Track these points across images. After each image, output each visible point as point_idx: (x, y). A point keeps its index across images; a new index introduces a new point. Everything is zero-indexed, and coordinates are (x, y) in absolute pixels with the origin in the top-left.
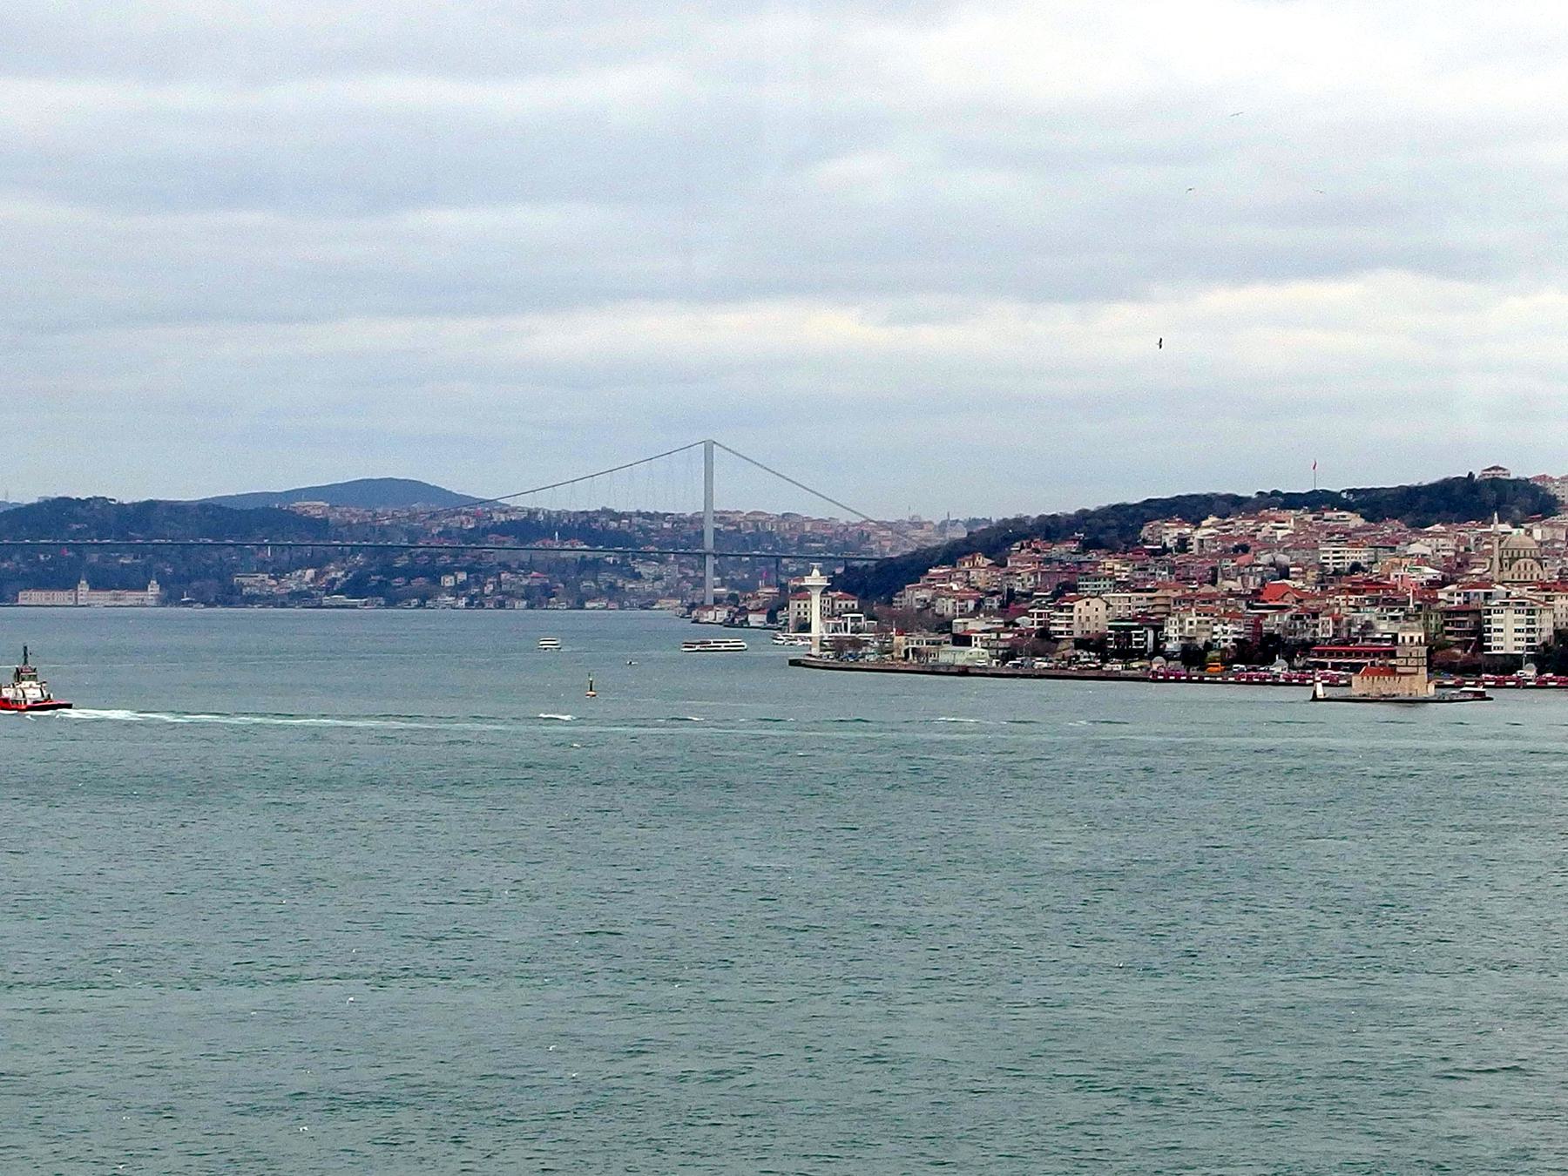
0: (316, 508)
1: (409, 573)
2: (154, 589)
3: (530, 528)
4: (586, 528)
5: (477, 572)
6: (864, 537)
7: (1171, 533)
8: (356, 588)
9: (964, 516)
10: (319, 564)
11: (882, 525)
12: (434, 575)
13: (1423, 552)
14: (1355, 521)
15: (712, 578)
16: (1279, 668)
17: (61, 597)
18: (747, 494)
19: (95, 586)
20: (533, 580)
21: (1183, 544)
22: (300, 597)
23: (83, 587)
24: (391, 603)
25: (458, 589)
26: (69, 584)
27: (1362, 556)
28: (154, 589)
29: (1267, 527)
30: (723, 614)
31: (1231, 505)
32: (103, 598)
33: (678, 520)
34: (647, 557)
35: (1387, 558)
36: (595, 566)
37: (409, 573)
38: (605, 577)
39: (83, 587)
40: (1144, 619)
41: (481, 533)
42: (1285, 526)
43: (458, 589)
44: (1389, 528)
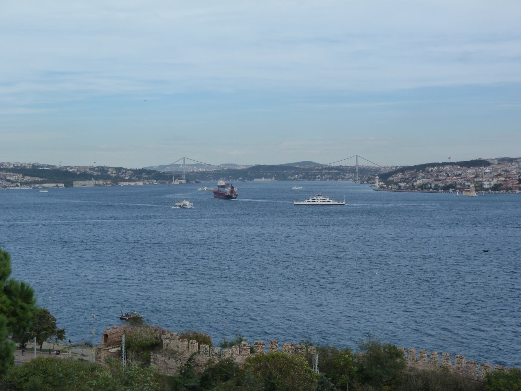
0: (297, 166)
1: (311, 175)
2: (273, 178)
3: (330, 168)
4: (337, 168)
5: (322, 175)
6: (380, 169)
7: (430, 169)
8: (304, 178)
9: (394, 166)
10: (298, 174)
11: (382, 167)
12: (315, 176)
14: (459, 167)
15: (357, 176)
16: (451, 190)
17: (259, 180)
18: (362, 163)
19: (265, 178)
20: (330, 176)
21: (432, 171)
22: (295, 179)
23: (263, 178)
24: (309, 179)
25: (319, 178)
26: (261, 178)
27: (460, 172)
28: (273, 178)
29: (445, 169)
30: (359, 182)
31: (438, 165)
32: (266, 180)
33: (351, 167)
34: (347, 173)
35: (465, 173)
36: (339, 174)
37: (311, 175)
38: (341, 176)
39: (263, 178)
40: (429, 183)
41: (322, 169)
42: (448, 168)
43: (319, 178)
44: (465, 168)
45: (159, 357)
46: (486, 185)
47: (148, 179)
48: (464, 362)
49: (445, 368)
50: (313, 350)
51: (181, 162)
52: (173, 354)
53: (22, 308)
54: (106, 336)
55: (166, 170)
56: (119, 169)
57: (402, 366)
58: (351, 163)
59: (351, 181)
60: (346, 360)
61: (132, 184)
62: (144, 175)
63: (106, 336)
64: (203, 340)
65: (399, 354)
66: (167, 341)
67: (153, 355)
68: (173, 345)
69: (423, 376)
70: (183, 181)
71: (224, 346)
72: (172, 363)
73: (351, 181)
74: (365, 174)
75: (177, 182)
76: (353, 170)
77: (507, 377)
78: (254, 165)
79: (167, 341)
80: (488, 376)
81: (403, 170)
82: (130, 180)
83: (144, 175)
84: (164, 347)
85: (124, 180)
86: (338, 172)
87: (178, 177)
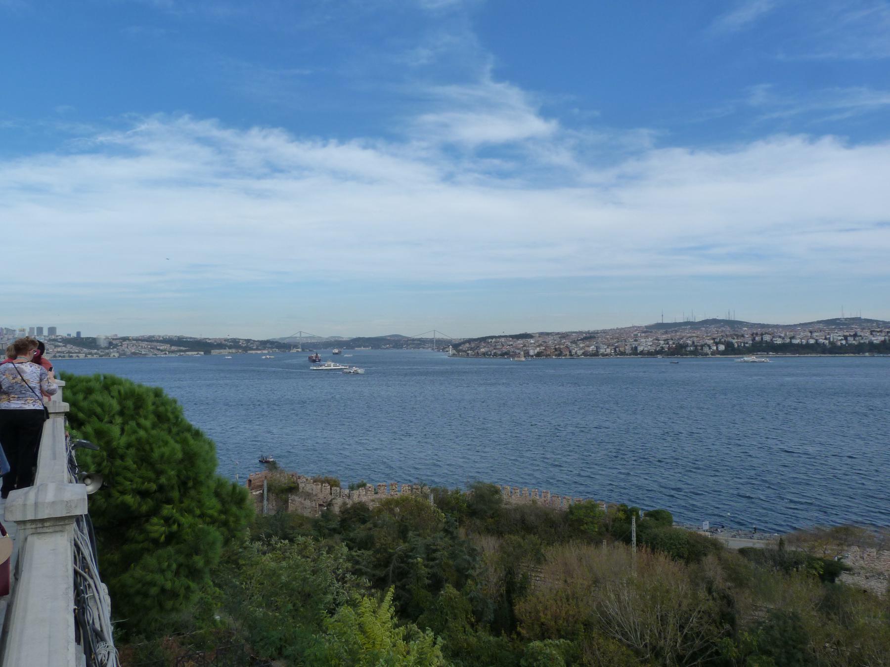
3: (414, 340)
4: (419, 340)
5: (408, 345)
8: (394, 347)
13: (520, 341)
18: (438, 336)
36: (420, 344)
42: (503, 340)
45: (296, 498)
46: (531, 353)
47: (272, 348)
48: (549, 496)
49: (534, 502)
50: (427, 490)
51: (298, 335)
52: (308, 496)
53: (236, 516)
54: (250, 481)
55: (285, 342)
56: (248, 341)
57: (500, 501)
58: (430, 336)
59: (430, 350)
60: (458, 499)
61: (259, 352)
62: (268, 345)
63: (250, 481)
64: (333, 484)
65: (497, 491)
66: (303, 485)
67: (291, 497)
68: (308, 488)
69: (517, 509)
70: (300, 350)
71: (352, 488)
72: (308, 503)
73: (430, 350)
74: (441, 344)
75: (295, 350)
76: (431, 341)
77: (586, 507)
78: (354, 337)
79: (303, 485)
80: (570, 507)
81: (469, 341)
82: (257, 349)
83: (268, 345)
84: (301, 490)
85: (252, 349)
86: (421, 343)
87: (296, 346)
